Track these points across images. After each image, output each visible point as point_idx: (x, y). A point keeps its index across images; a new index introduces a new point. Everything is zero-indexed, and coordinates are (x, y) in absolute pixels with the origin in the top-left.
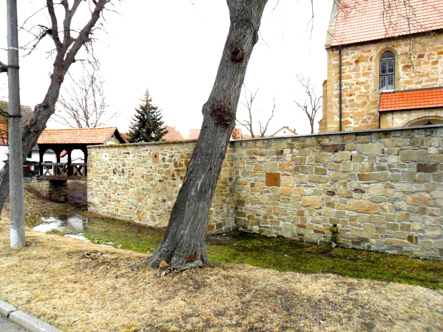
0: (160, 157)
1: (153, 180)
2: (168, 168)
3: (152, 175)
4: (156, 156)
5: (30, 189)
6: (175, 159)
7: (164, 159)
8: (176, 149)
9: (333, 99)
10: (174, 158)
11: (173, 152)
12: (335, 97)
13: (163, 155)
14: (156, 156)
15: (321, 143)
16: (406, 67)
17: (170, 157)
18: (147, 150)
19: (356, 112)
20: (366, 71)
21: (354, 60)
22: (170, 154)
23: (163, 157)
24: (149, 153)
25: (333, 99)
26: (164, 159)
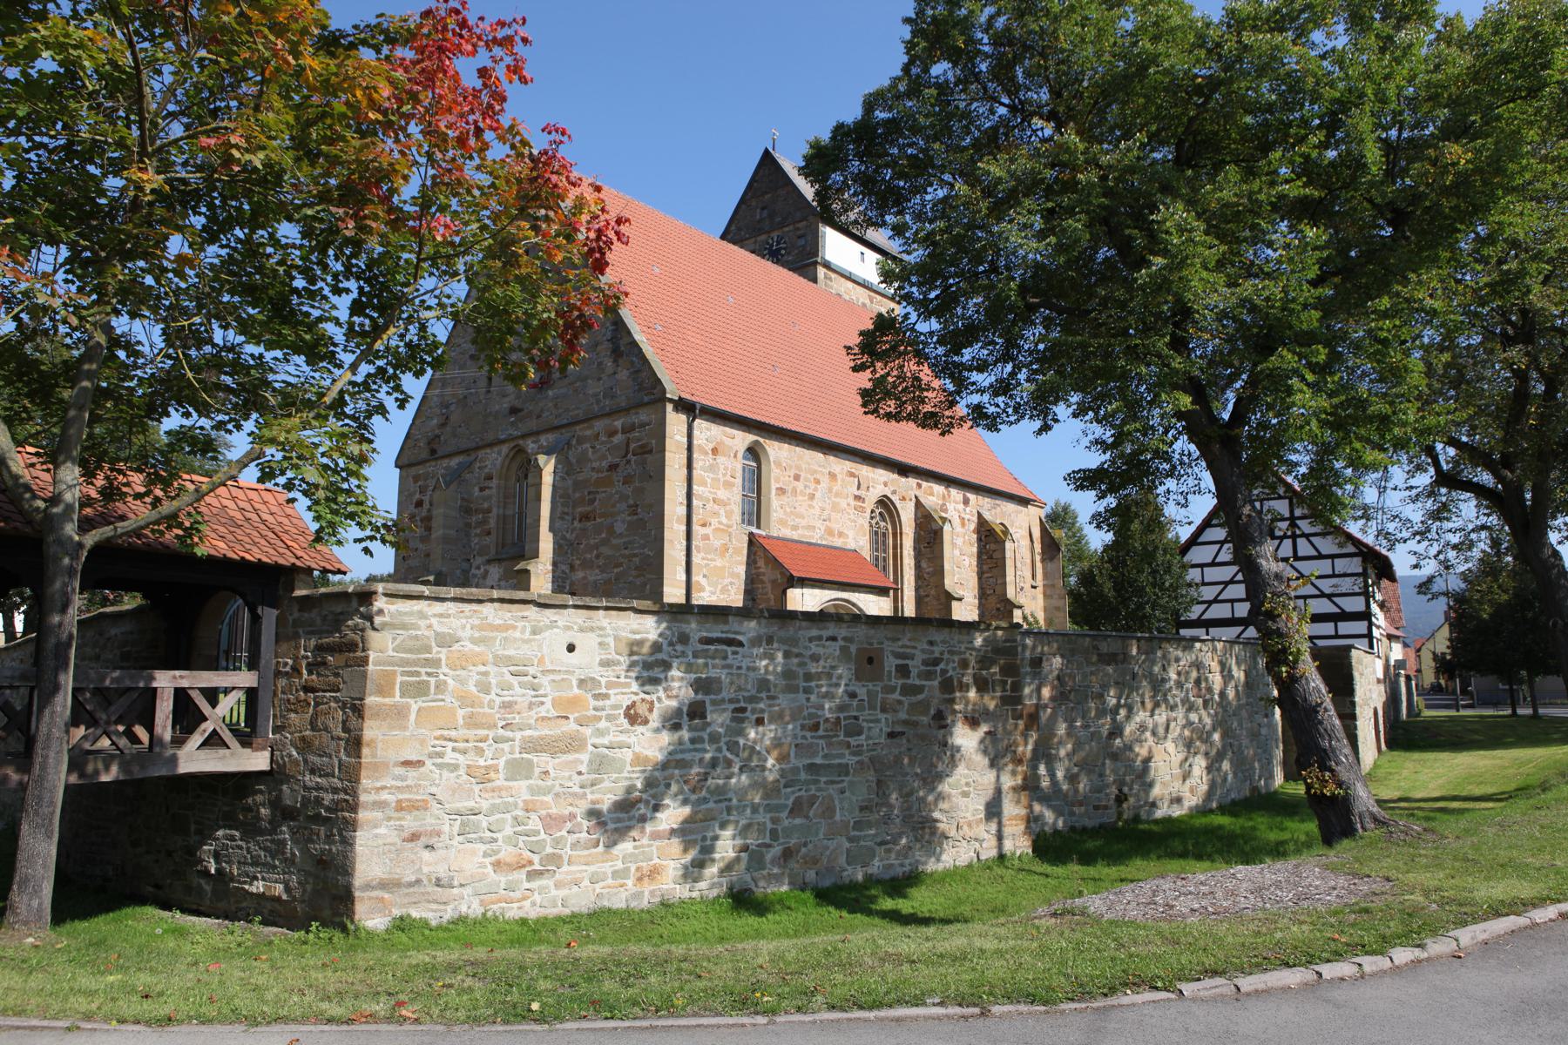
0: (890, 663)
1: (860, 733)
2: (920, 697)
3: (856, 718)
4: (870, 661)
5: (656, 836)
6: (944, 672)
7: (903, 671)
8: (944, 642)
9: (676, 526)
10: (942, 666)
11: (937, 650)
12: (678, 521)
13: (898, 656)
14: (870, 661)
15: (648, 628)
16: (781, 491)
17: (925, 663)
18: (834, 639)
19: (712, 564)
20: (728, 478)
21: (711, 446)
22: (926, 656)
23: (900, 662)
24: (844, 650)
25: (676, 526)
26: (903, 671)
